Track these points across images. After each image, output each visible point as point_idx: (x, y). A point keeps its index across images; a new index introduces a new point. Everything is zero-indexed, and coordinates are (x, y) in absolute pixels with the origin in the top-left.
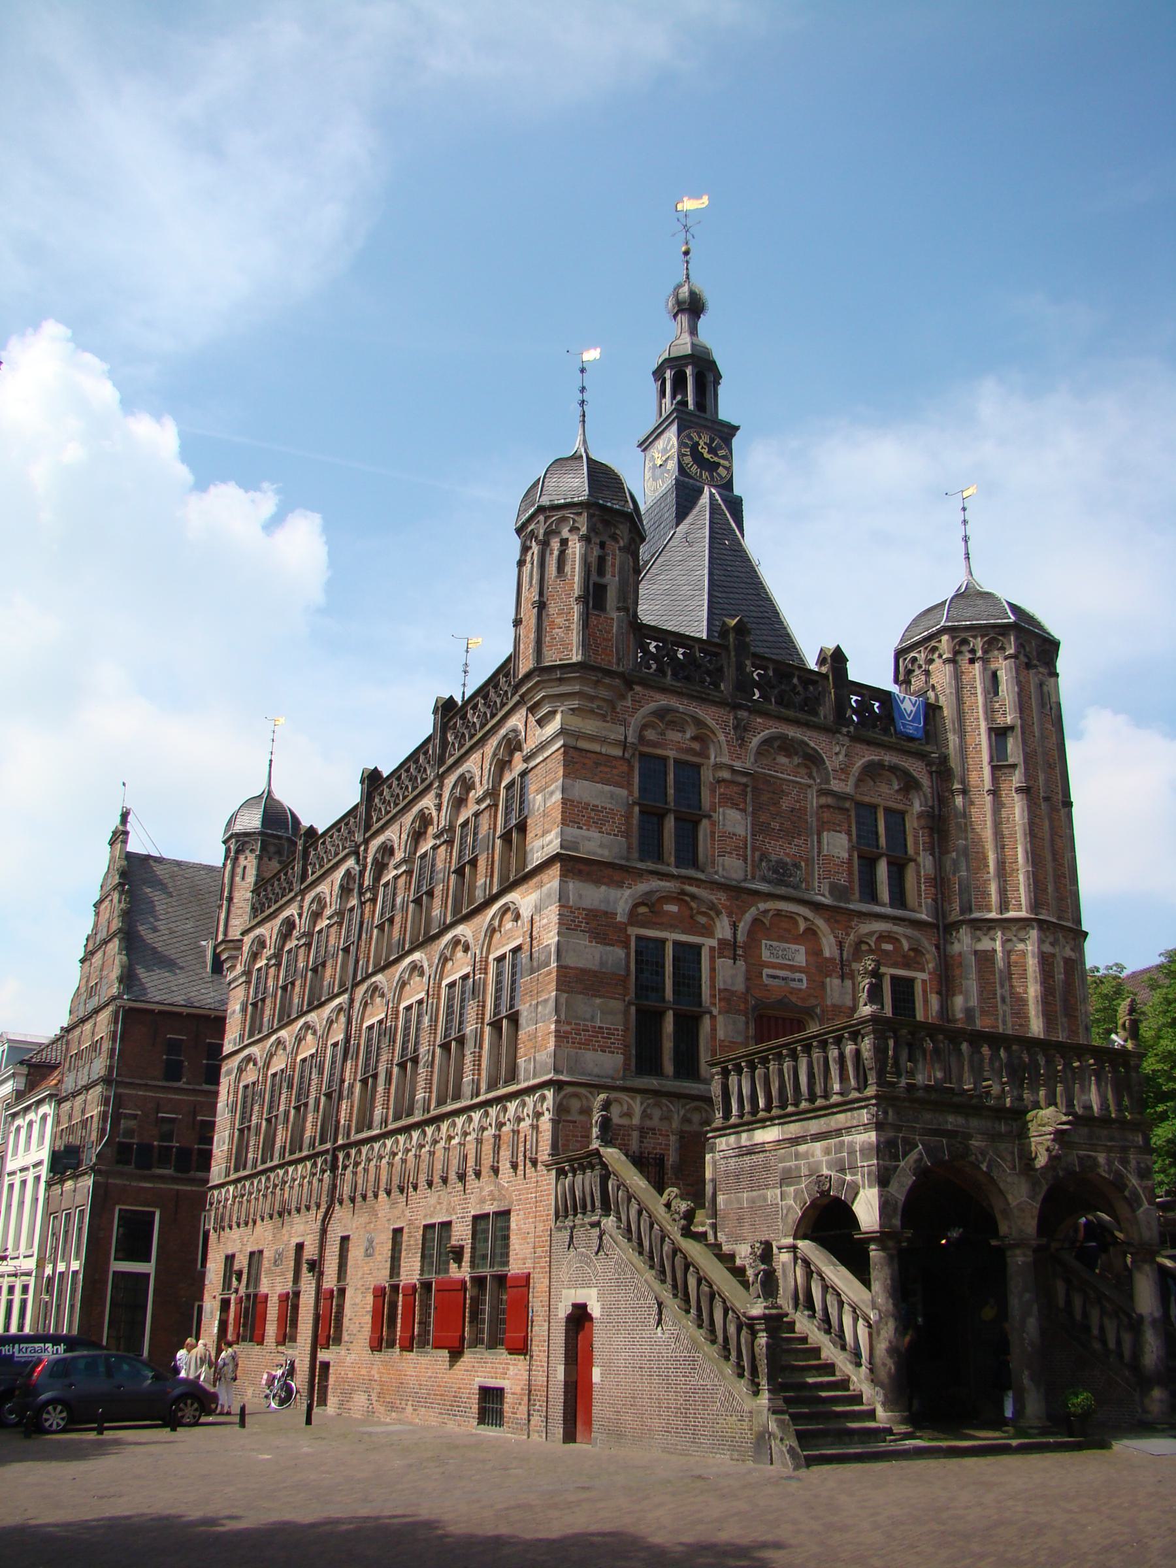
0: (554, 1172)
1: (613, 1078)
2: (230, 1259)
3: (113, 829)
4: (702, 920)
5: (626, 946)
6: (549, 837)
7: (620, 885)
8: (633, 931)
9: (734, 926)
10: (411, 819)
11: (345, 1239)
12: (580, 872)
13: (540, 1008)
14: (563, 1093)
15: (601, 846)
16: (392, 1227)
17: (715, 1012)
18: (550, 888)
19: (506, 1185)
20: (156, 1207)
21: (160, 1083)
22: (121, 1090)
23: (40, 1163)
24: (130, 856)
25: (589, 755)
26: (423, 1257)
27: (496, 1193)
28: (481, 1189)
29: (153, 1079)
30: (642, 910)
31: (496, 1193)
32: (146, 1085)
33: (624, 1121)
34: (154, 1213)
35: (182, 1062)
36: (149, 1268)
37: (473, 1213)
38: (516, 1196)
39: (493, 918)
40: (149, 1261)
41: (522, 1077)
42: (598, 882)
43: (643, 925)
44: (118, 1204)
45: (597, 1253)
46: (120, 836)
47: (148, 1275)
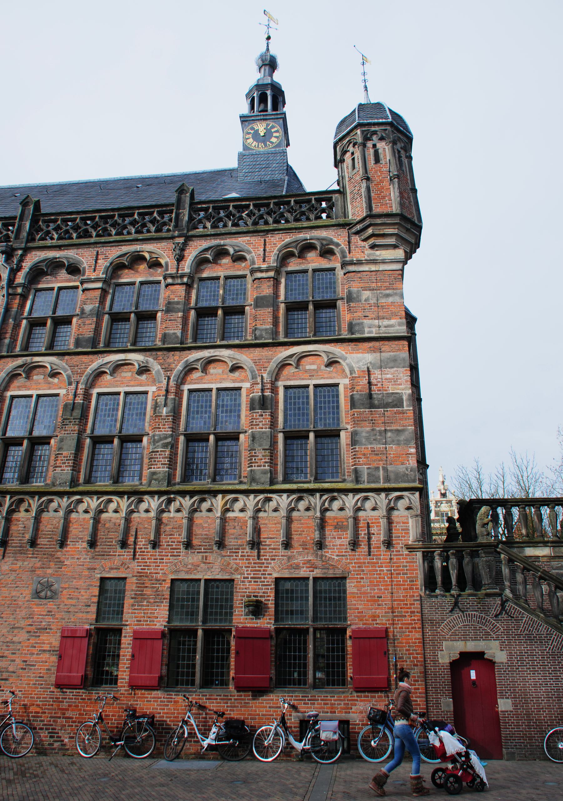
0: (419, 555)
6: (386, 322)
10: (119, 253)
13: (389, 434)
16: (99, 576)
18: (395, 356)
19: (336, 558)
26: (171, 607)
27: (319, 563)
28: (289, 558)
31: (319, 563)
37: (275, 575)
38: (353, 567)
39: (291, 356)
41: (365, 477)
45: (496, 616)
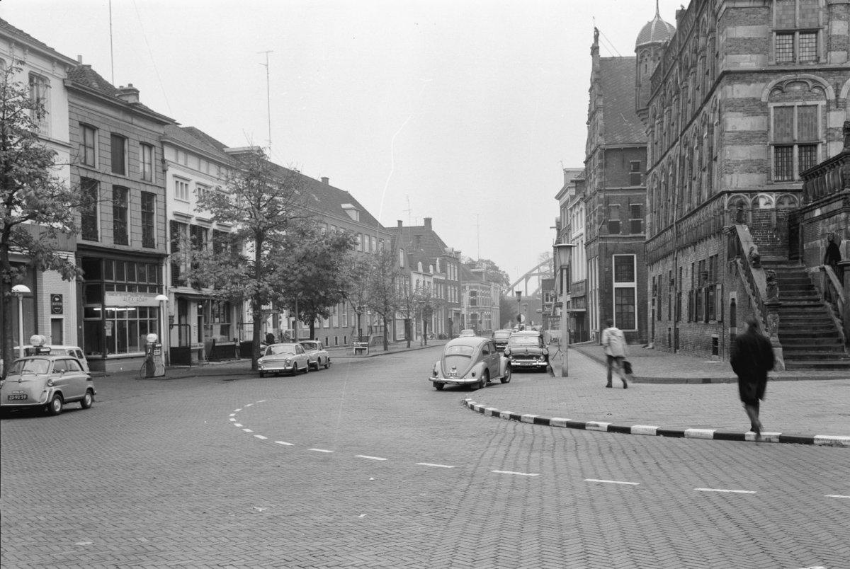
1: (759, 186)
2: (654, 278)
3: (591, 46)
4: (816, 91)
5: (767, 114)
7: (764, 81)
8: (771, 105)
9: (837, 92)
11: (681, 268)
12: (738, 78)
14: (731, 197)
15: (751, 61)
17: (825, 142)
20: (634, 253)
21: (628, 188)
22: (607, 195)
23: (582, 235)
24: (604, 61)
25: (743, 10)
29: (626, 185)
30: (777, 92)
32: (621, 189)
33: (768, 207)
34: (633, 256)
35: (640, 174)
36: (634, 285)
40: (633, 281)
42: (749, 83)
43: (777, 101)
44: (614, 253)
46: (595, 50)
47: (633, 288)
